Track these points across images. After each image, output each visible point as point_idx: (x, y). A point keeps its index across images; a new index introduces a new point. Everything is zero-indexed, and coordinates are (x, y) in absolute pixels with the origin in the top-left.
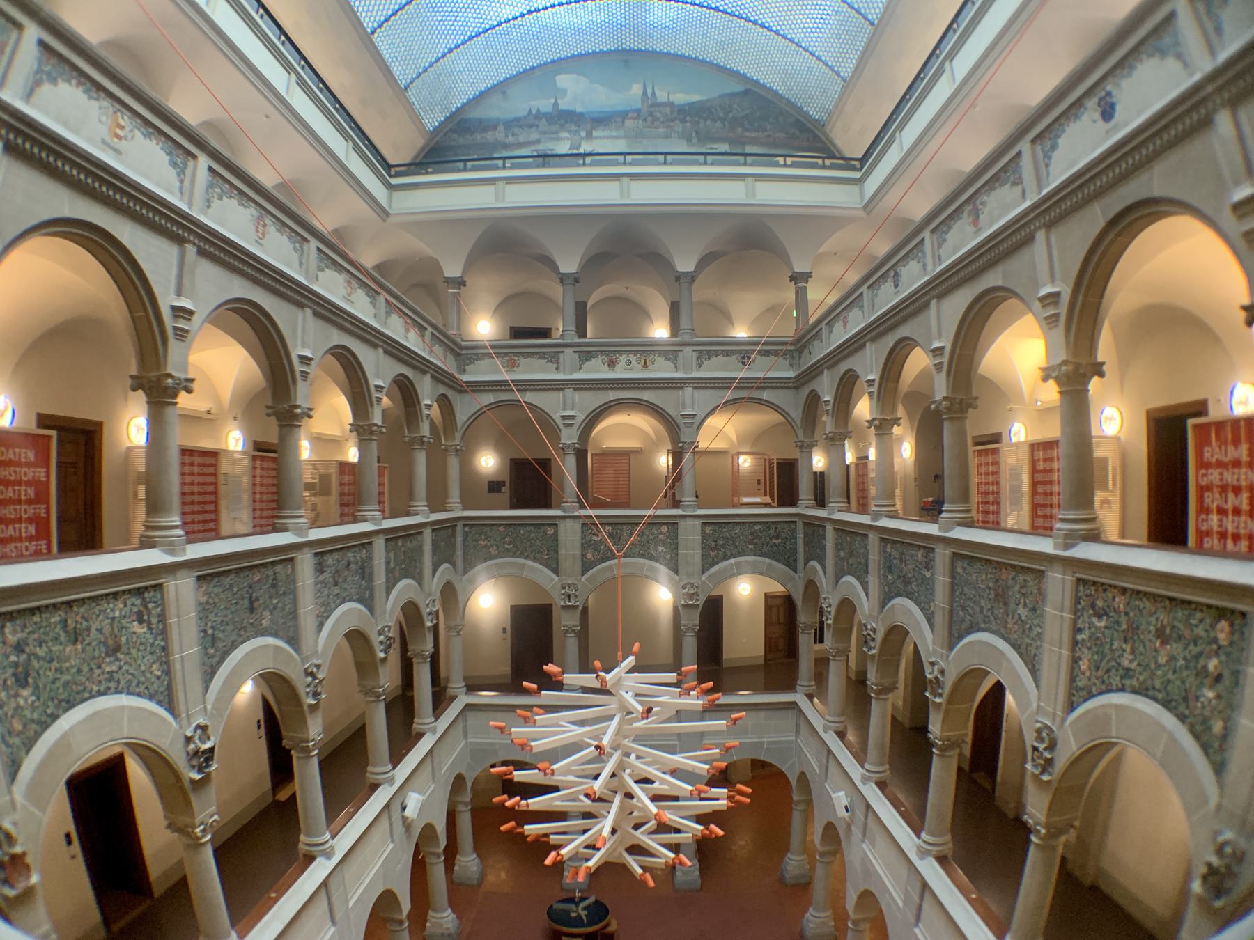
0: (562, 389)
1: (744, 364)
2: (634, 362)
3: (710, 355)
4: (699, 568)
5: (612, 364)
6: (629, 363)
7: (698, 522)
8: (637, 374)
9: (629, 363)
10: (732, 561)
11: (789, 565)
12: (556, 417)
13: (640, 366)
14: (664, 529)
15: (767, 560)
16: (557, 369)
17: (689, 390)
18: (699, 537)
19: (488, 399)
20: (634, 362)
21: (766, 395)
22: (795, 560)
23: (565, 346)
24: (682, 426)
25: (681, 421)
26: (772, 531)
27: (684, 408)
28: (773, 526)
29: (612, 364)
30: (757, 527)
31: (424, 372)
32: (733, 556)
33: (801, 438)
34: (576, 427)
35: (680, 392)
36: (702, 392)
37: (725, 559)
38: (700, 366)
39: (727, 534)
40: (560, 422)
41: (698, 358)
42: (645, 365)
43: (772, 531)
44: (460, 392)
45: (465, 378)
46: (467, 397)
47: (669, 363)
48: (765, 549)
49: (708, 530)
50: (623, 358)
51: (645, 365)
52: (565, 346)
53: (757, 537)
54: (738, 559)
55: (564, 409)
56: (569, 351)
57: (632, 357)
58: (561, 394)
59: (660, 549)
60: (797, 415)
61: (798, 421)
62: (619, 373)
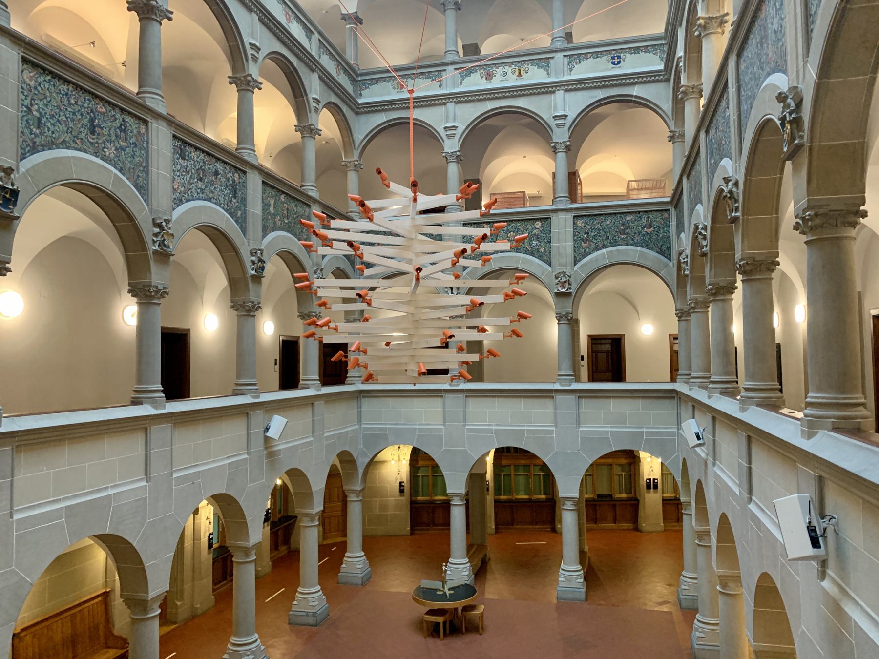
0: (445, 104)
1: (613, 63)
2: (510, 74)
3: (580, 58)
4: (571, 259)
5: (489, 76)
6: (504, 74)
7: (570, 216)
8: (512, 81)
9: (504, 74)
10: (604, 251)
11: (662, 253)
12: (441, 130)
13: (515, 76)
14: (538, 224)
15: (639, 248)
16: (440, 86)
17: (560, 94)
18: (570, 230)
19: (381, 118)
20: (510, 74)
21: (636, 91)
22: (669, 248)
23: (447, 64)
24: (554, 127)
25: (552, 123)
26: (644, 221)
27: (556, 110)
28: (645, 216)
29: (489, 76)
30: (629, 217)
31: (313, 71)
32: (605, 246)
33: (673, 129)
34: (457, 137)
35: (552, 96)
36: (573, 93)
37: (597, 249)
38: (571, 70)
39: (598, 226)
40: (443, 133)
41: (569, 63)
42: (520, 75)
43: (644, 221)
44: (357, 113)
45: (360, 101)
46: (363, 118)
47: (542, 70)
48: (637, 238)
49: (580, 223)
50: (500, 70)
51: (520, 75)
52: (447, 64)
53: (628, 227)
54: (609, 249)
55: (447, 122)
56: (450, 68)
57: (508, 69)
58: (443, 108)
59: (534, 243)
60: (667, 106)
61: (670, 113)
62: (497, 82)
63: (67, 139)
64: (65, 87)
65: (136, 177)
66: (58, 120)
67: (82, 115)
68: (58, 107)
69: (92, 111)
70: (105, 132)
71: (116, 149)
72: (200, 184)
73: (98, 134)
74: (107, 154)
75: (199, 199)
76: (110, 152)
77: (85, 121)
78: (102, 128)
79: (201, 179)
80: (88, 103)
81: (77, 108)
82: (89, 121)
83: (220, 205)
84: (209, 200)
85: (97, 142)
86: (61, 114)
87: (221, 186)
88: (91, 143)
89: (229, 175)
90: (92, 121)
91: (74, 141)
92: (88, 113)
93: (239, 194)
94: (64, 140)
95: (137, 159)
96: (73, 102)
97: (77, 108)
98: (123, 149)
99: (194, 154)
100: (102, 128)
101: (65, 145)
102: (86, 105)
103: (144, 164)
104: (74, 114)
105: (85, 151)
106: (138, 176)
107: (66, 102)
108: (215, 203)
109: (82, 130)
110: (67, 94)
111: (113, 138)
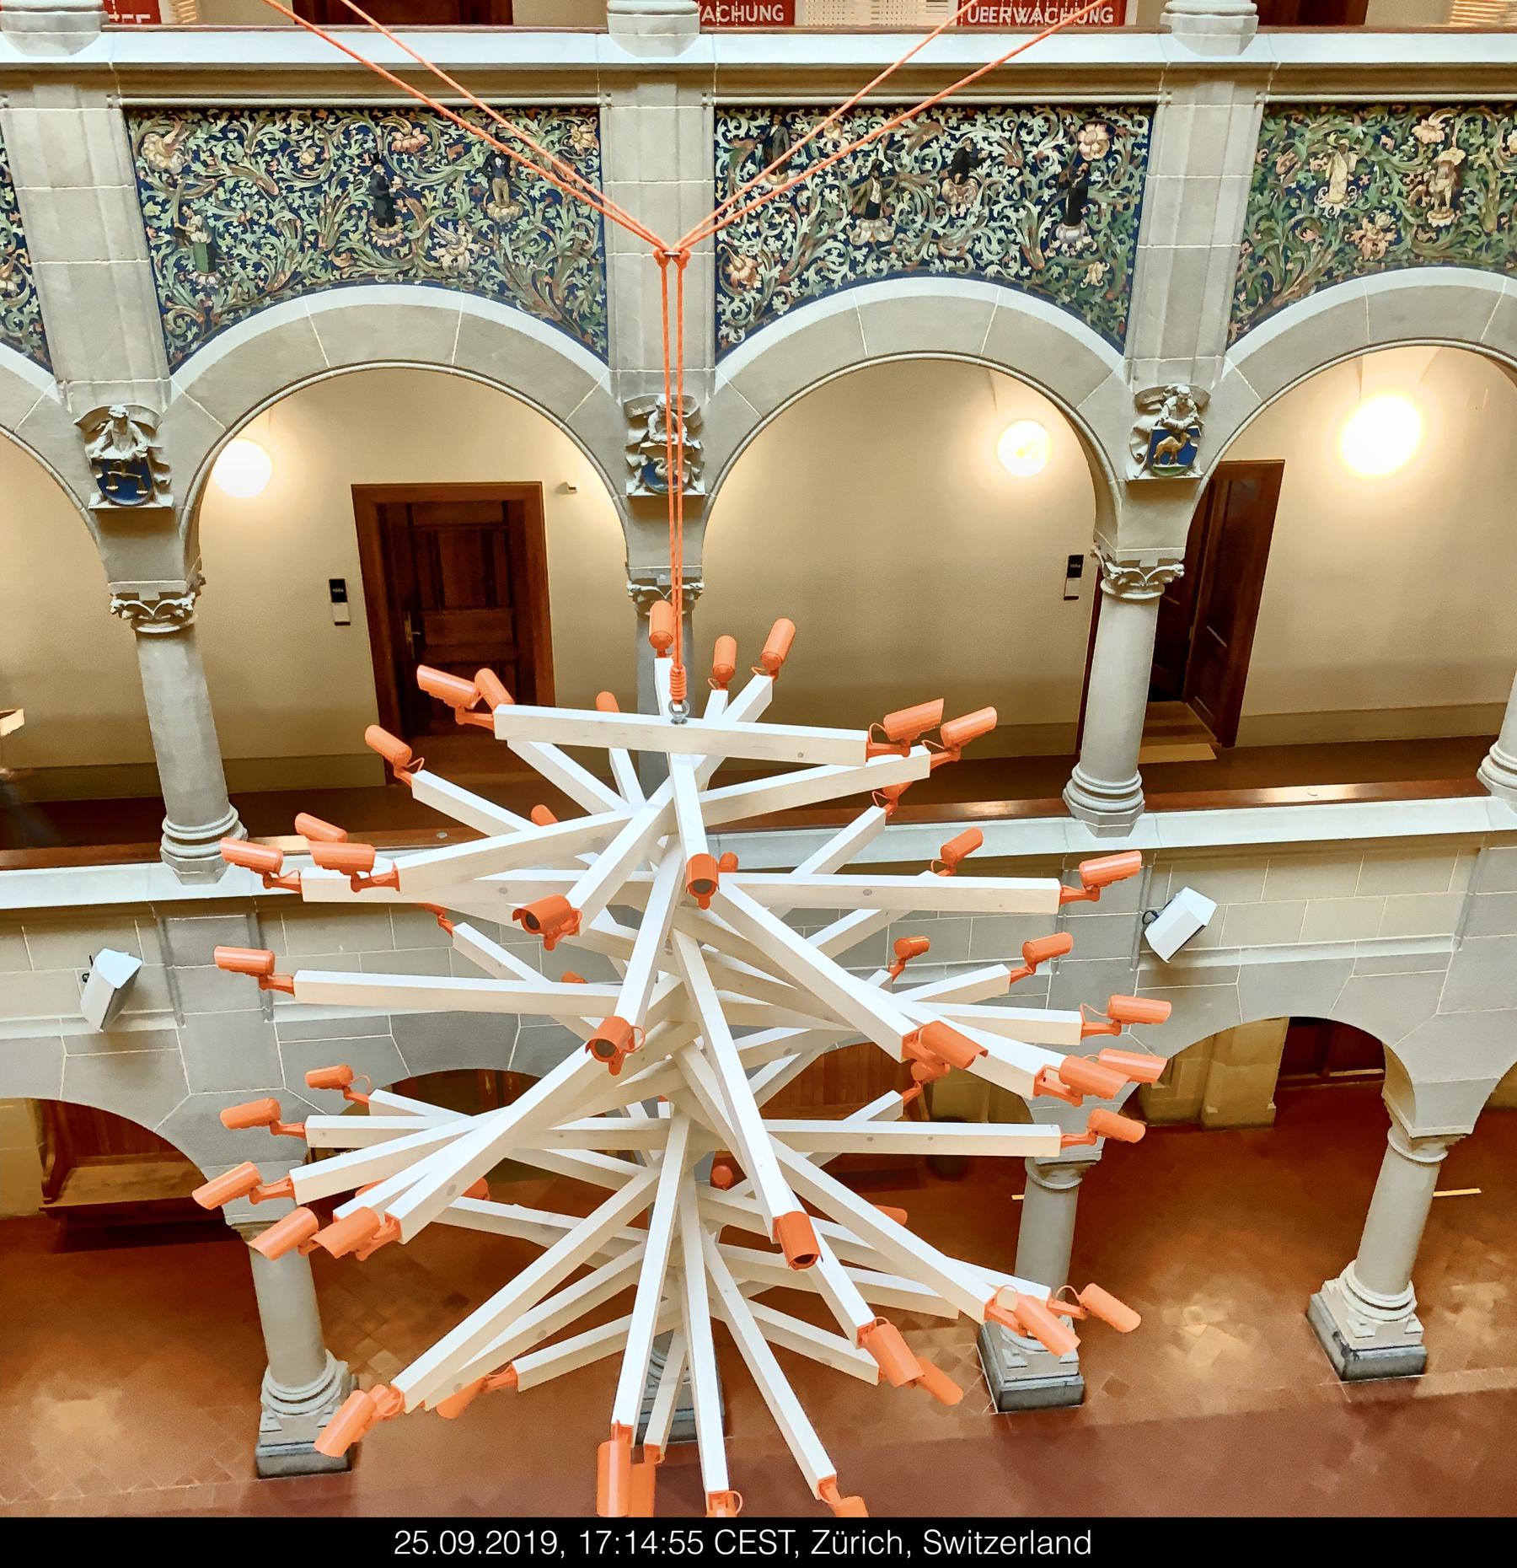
63: (304, 268)
64: (276, 130)
65: (561, 293)
66: (269, 228)
67: (343, 183)
68: (264, 193)
69: (376, 160)
70: (429, 202)
71: (480, 235)
72: (866, 231)
73: (409, 216)
74: (446, 261)
75: (863, 280)
76: (458, 249)
77: (357, 196)
78: (419, 196)
79: (872, 212)
80: (349, 147)
81: (322, 172)
82: (371, 191)
83: (978, 274)
84: (923, 268)
85: (405, 241)
86: (275, 207)
87: (988, 201)
88: (386, 251)
89: (1046, 147)
90: (381, 186)
91: (327, 265)
92: (364, 170)
93: (1103, 199)
94: (295, 274)
95: (563, 241)
96: (307, 158)
97: (322, 172)
98: (499, 227)
99: (834, 135)
100: (419, 196)
101: (300, 284)
102: (354, 150)
103: (594, 246)
104: (318, 189)
105: (369, 280)
106: (572, 288)
107: (286, 168)
108: (952, 273)
109: (348, 225)
110: (285, 145)
111: (464, 205)
